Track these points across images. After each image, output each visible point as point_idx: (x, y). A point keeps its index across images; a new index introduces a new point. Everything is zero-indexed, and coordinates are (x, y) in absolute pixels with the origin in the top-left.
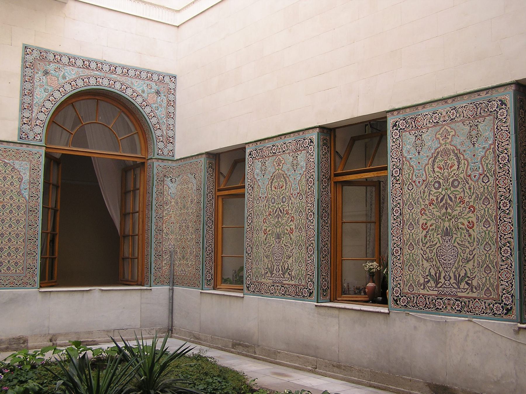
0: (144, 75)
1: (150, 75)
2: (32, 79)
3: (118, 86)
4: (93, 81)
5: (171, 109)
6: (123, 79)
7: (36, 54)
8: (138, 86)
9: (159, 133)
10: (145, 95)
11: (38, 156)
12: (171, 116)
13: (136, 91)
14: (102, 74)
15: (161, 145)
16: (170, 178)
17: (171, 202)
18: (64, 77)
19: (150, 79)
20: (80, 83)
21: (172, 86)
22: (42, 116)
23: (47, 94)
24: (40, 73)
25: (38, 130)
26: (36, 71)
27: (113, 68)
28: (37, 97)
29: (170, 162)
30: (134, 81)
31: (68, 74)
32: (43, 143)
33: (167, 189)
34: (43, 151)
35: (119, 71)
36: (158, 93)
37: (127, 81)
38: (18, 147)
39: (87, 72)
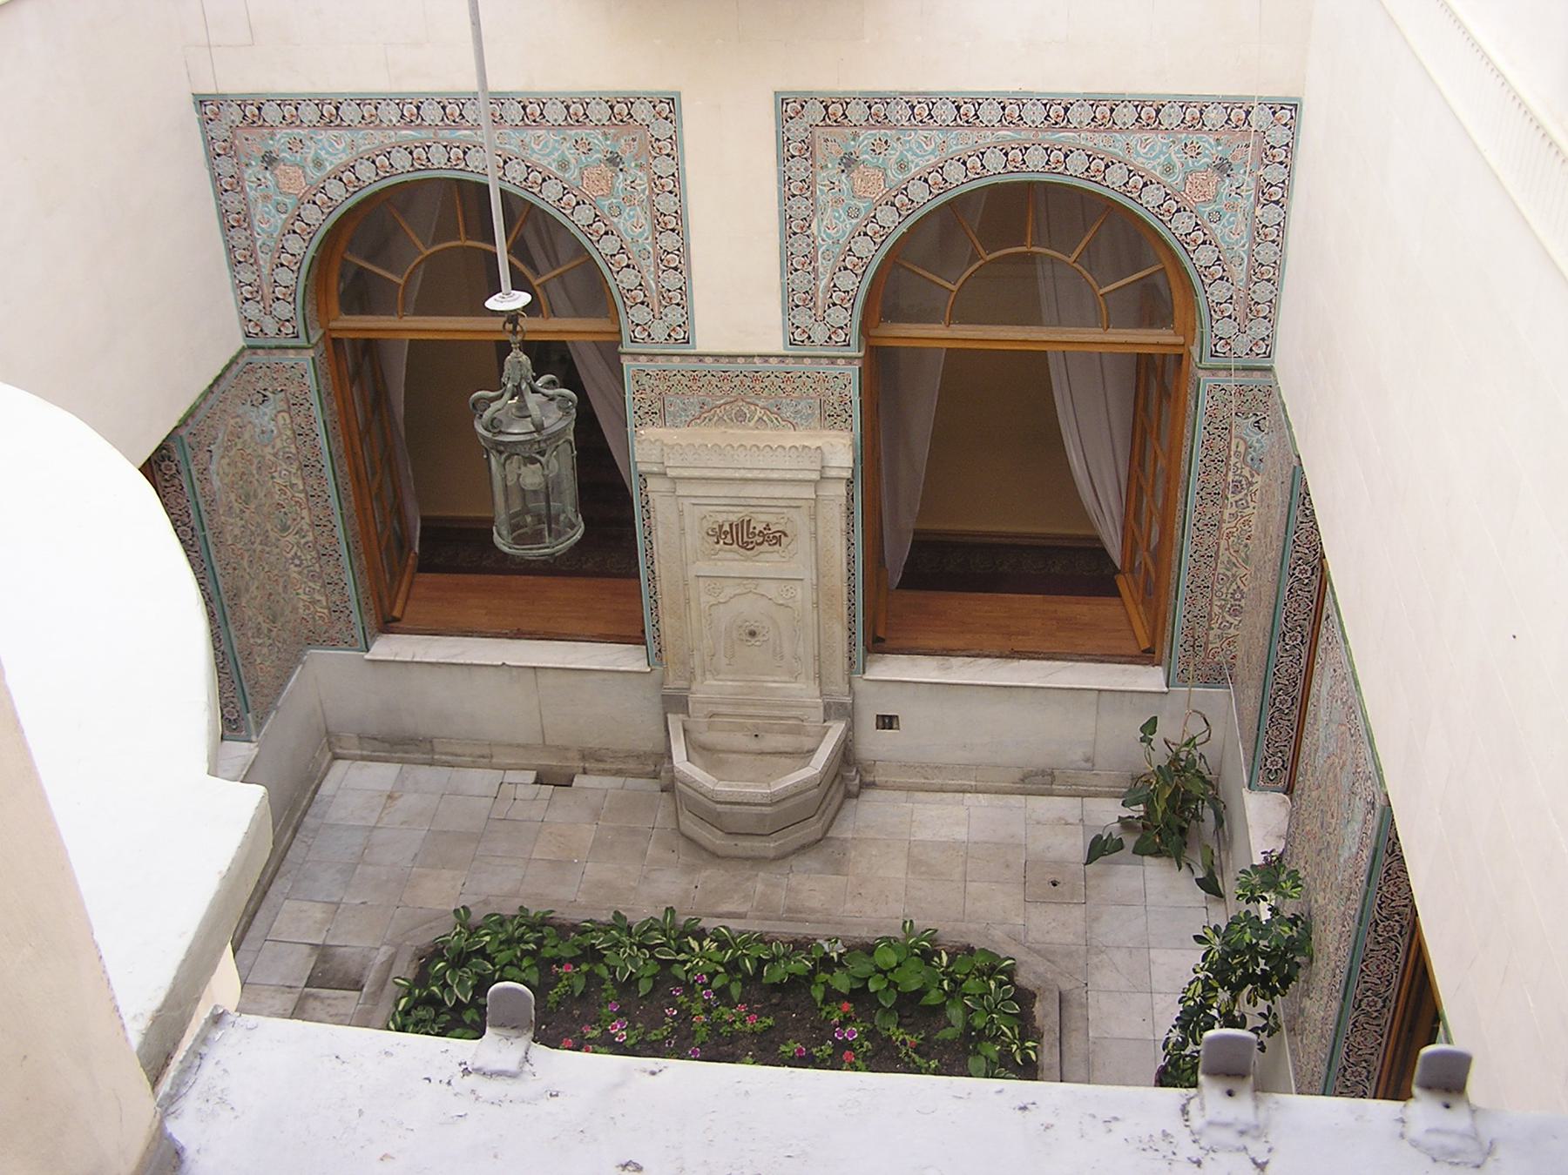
0: (1171, 117)
1: (1193, 114)
2: (808, 185)
3: (1077, 163)
4: (994, 161)
5: (1270, 214)
6: (1100, 140)
7: (815, 113)
8: (1150, 153)
9: (1219, 292)
10: (1175, 180)
11: (840, 382)
12: (1271, 235)
13: (1143, 172)
14: (1025, 135)
15: (1225, 328)
16: (1254, 419)
17: (1251, 484)
18: (902, 166)
19: (1198, 124)
20: (955, 173)
21: (1279, 135)
22: (847, 281)
23: (854, 221)
24: (833, 169)
25: (838, 316)
26: (820, 161)
27: (1057, 111)
28: (829, 236)
29: (1257, 374)
30: (1134, 139)
31: (915, 154)
32: (853, 352)
33: (1242, 449)
34: (853, 372)
35: (1079, 115)
36: (1223, 167)
37: (1113, 145)
38: (790, 365)
39: (971, 135)
